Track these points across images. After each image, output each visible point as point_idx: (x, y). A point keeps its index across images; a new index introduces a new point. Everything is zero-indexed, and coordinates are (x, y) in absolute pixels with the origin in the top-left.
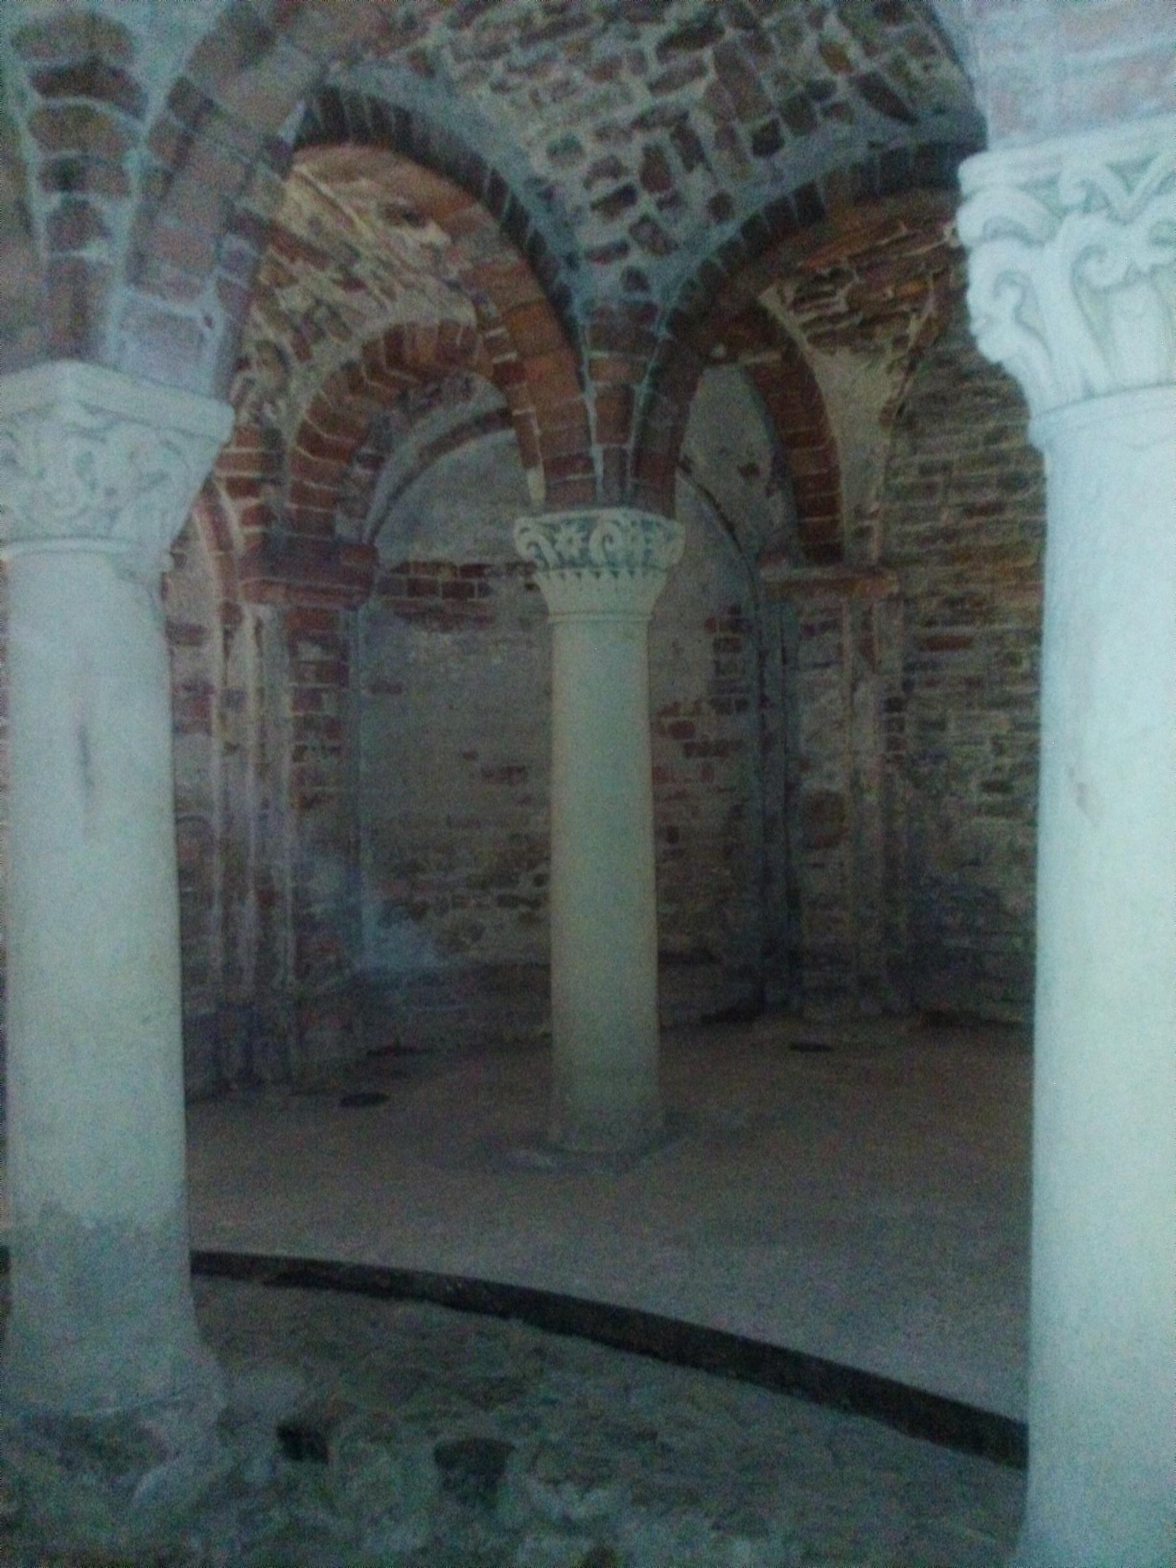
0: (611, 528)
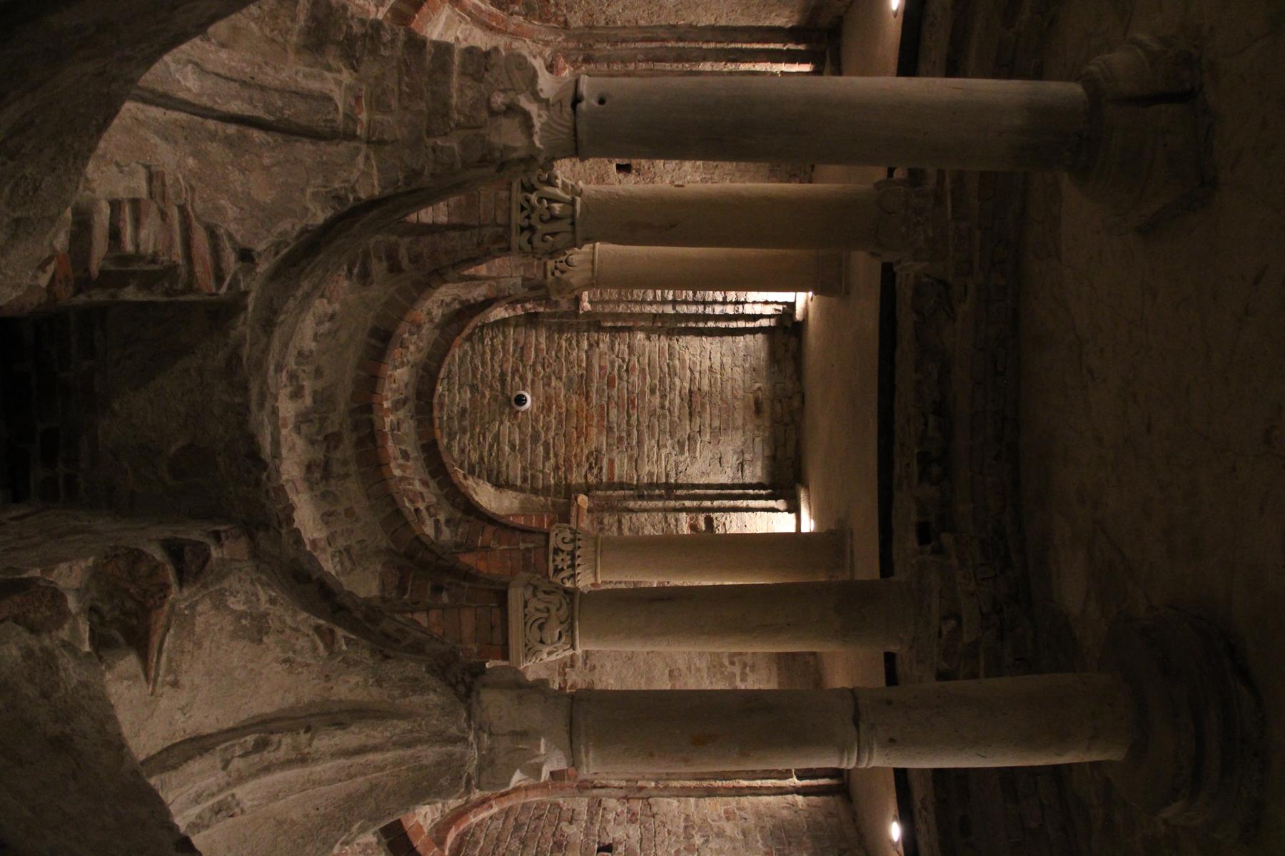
0: (559, 538)
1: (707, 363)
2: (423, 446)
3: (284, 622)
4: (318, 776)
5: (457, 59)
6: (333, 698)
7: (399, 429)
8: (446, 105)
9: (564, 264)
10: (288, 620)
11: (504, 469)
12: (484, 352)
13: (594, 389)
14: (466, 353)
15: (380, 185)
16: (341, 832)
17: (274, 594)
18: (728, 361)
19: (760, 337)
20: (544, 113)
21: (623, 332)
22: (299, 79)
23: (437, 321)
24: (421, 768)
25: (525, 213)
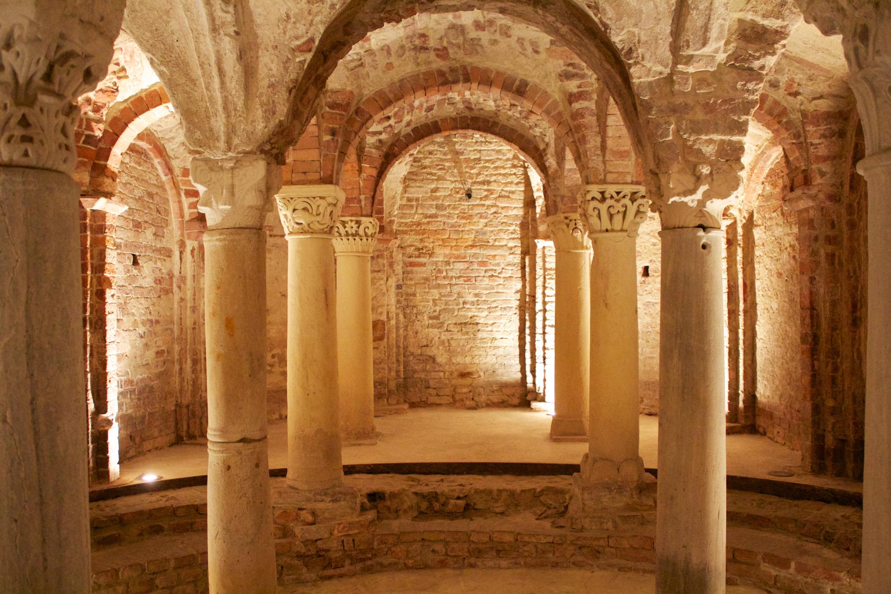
1: (498, 336)
2: (436, 122)
3: (317, 14)
4: (202, 41)
5: (735, 138)
6: (260, 52)
7: (449, 104)
8: (699, 132)
9: (574, 226)
10: (318, 18)
11: (418, 184)
12: (503, 168)
13: (478, 251)
14: (504, 155)
15: (641, 82)
16: (161, 59)
17: (337, 7)
18: (500, 352)
19: (519, 376)
20: (695, 204)
21: (522, 272)
22: (719, 21)
23: (531, 131)
24: (208, 117)
25: (615, 195)
